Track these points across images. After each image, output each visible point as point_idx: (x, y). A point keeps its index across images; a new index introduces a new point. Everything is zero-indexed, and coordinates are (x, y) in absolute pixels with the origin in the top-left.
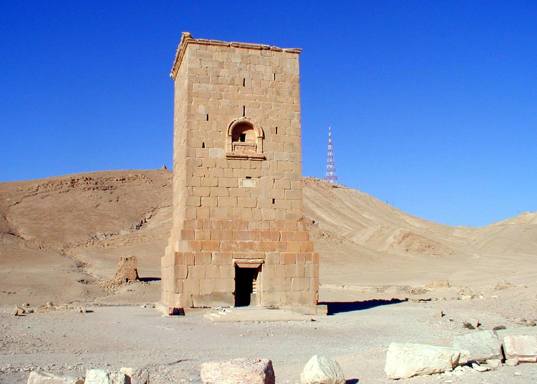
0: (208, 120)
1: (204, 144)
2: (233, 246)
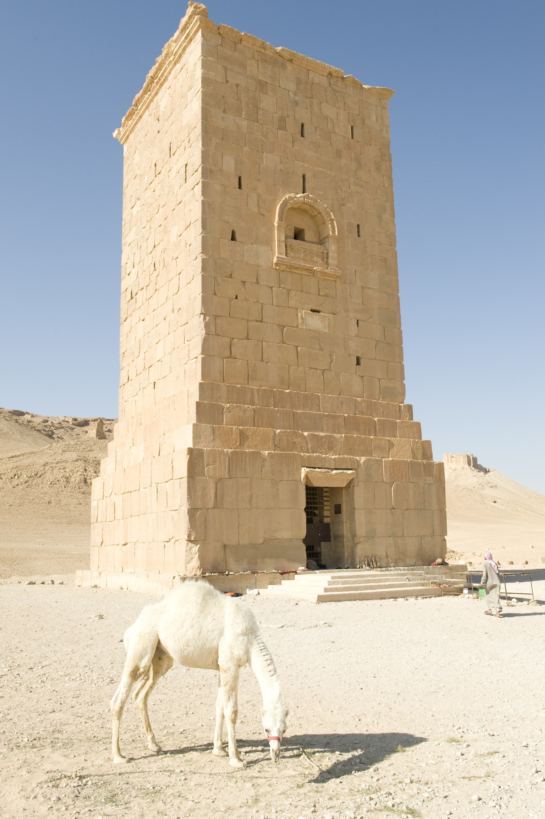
0: (240, 187)
1: (233, 233)
2: (298, 440)
